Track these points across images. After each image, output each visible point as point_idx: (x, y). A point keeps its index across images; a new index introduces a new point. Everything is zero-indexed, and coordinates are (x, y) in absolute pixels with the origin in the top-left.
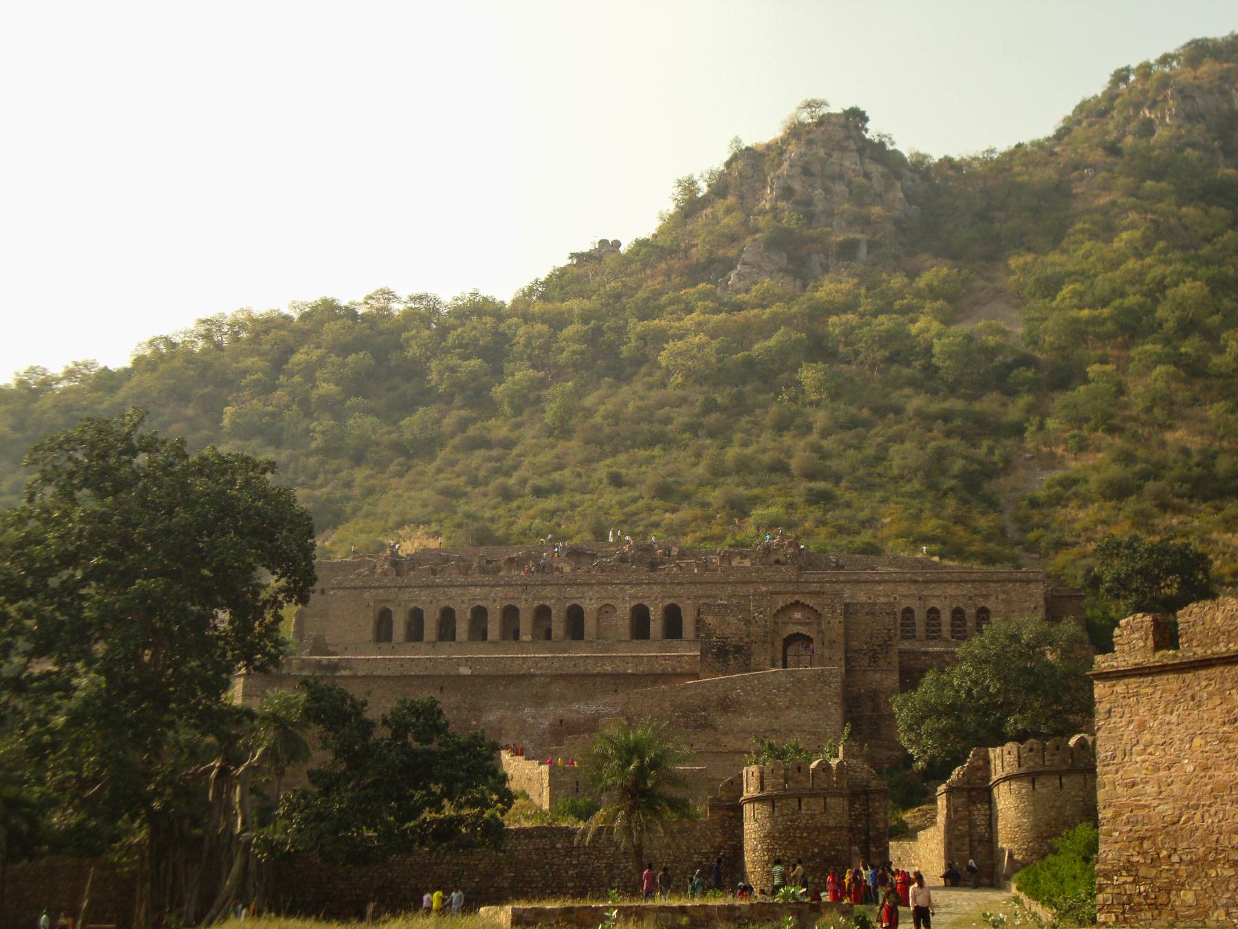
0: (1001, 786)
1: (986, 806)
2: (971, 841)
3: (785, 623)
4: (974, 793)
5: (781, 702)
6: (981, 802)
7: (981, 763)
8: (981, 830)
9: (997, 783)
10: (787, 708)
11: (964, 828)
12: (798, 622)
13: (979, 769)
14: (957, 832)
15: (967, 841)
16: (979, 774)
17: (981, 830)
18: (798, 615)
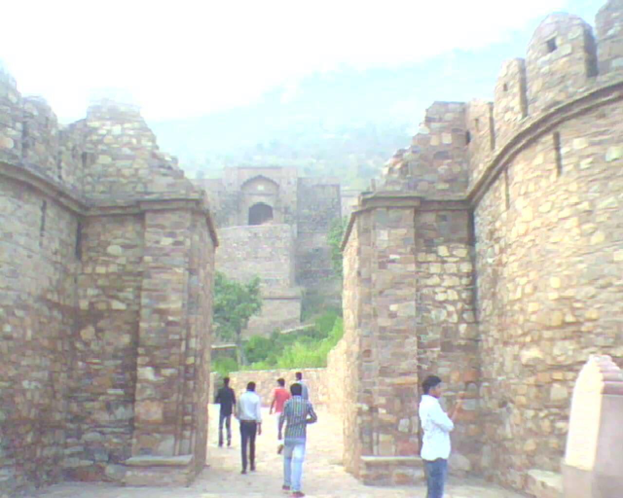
0: (519, 169)
1: (462, 251)
2: (420, 345)
3: (251, 194)
4: (429, 218)
5: (240, 255)
6: (447, 242)
7: (447, 139)
8: (448, 315)
9: (499, 169)
10: (245, 259)
11: (404, 310)
12: (261, 194)
13: (442, 154)
14: (383, 321)
15: (411, 345)
16: (443, 168)
17: (448, 315)
18: (261, 188)
